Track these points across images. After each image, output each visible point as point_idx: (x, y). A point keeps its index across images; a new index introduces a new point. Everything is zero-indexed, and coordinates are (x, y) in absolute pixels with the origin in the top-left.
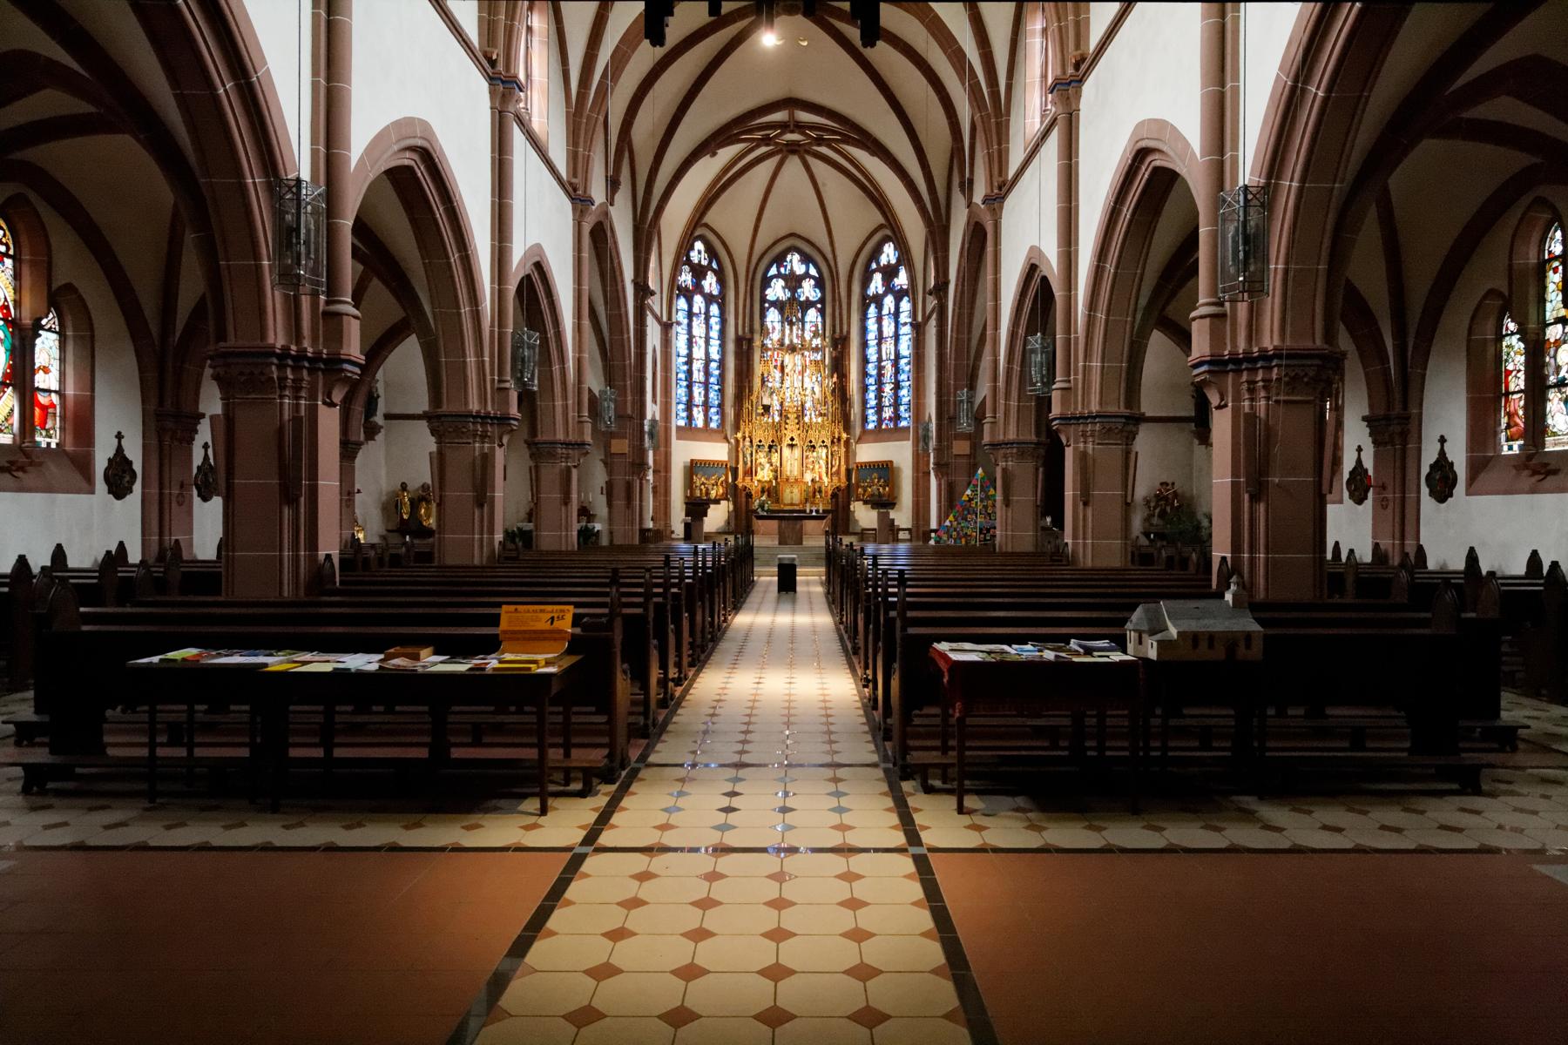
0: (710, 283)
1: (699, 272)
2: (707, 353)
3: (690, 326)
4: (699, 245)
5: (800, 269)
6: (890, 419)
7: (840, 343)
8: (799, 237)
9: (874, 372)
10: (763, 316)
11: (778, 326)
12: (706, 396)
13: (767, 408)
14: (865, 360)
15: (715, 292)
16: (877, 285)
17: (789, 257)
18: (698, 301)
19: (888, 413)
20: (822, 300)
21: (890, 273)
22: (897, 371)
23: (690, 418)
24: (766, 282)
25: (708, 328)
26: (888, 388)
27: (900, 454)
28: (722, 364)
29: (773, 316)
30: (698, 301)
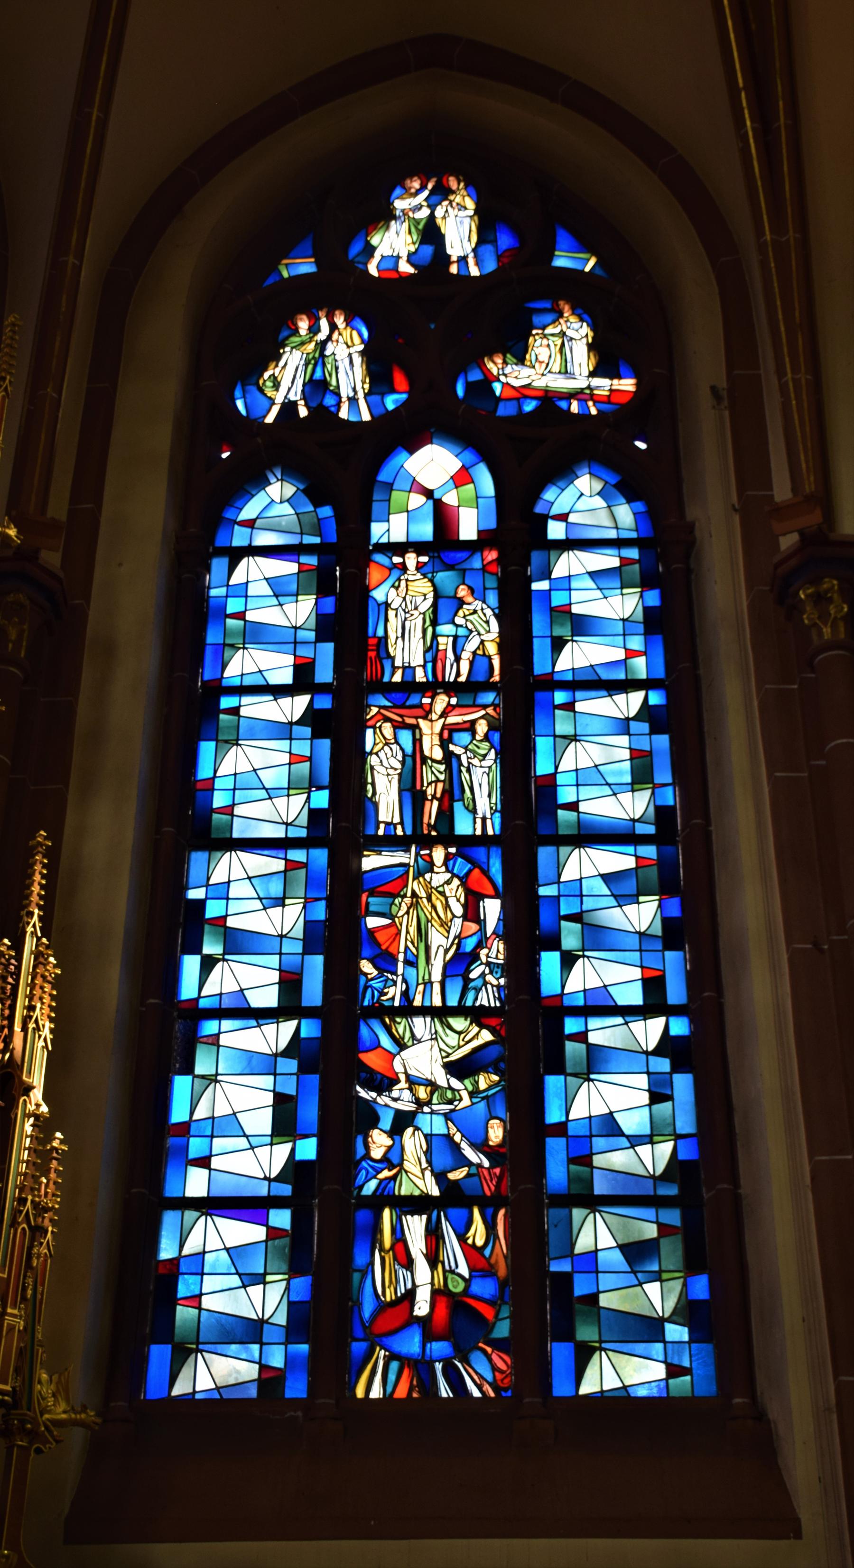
6: (458, 1318)
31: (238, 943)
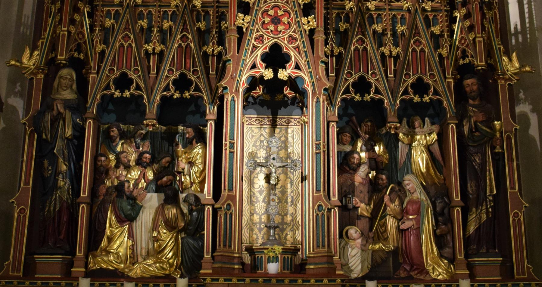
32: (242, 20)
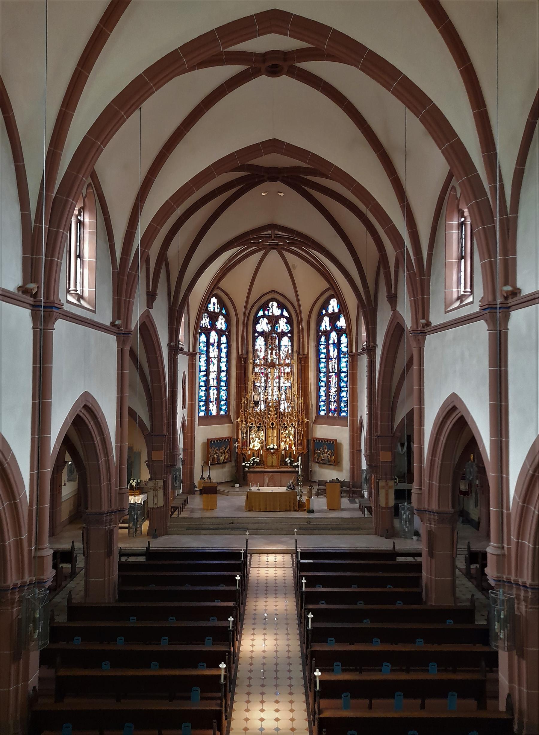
0: (221, 323)
1: (214, 317)
2: (219, 367)
3: (208, 352)
4: (214, 300)
5: (277, 312)
7: (303, 362)
8: (277, 292)
9: (324, 379)
10: (254, 339)
11: (264, 348)
12: (218, 394)
13: (257, 403)
14: (319, 371)
15: (224, 328)
16: (326, 323)
17: (271, 304)
18: (214, 336)
19: (333, 406)
20: (291, 332)
21: (334, 318)
22: (339, 380)
23: (208, 410)
24: (256, 321)
25: (220, 351)
26: (333, 390)
27: (341, 434)
28: (228, 372)
29: (260, 341)
30: (214, 336)
31: (322, 381)
32: (268, 419)
